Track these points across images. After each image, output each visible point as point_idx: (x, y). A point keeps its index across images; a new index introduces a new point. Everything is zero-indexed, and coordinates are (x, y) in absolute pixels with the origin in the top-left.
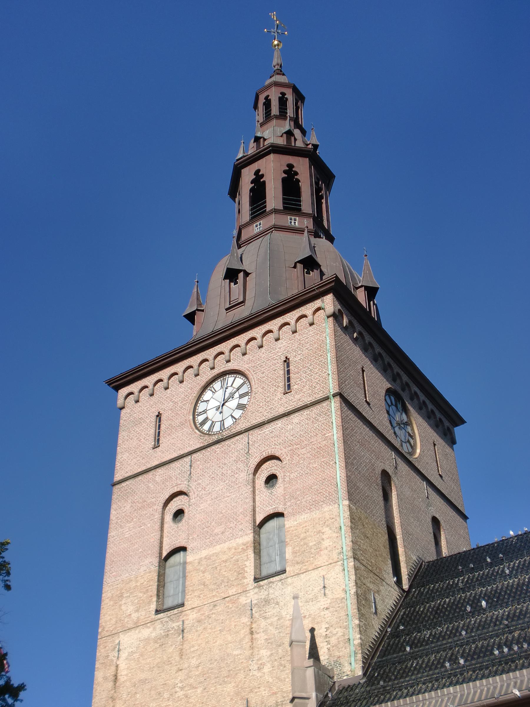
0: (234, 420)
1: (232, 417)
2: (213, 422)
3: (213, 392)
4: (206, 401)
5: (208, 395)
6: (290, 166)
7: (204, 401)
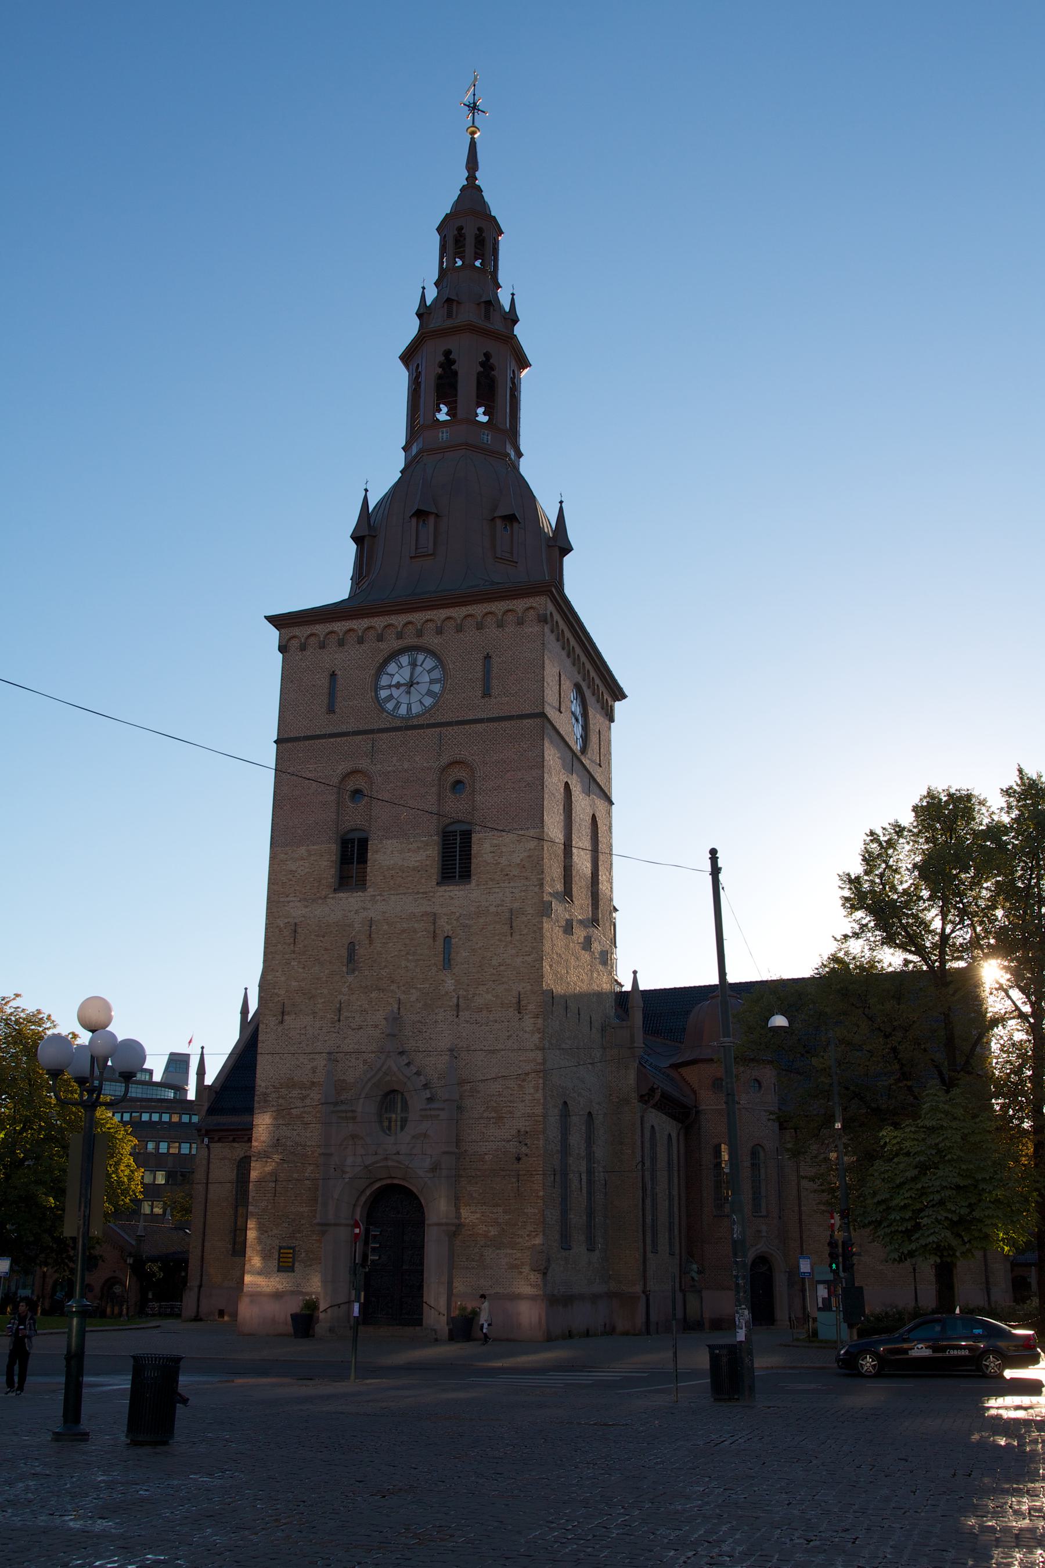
0: (424, 708)
1: (421, 702)
2: (398, 702)
3: (399, 666)
4: (391, 675)
5: (392, 668)
6: (487, 356)
7: (388, 674)
